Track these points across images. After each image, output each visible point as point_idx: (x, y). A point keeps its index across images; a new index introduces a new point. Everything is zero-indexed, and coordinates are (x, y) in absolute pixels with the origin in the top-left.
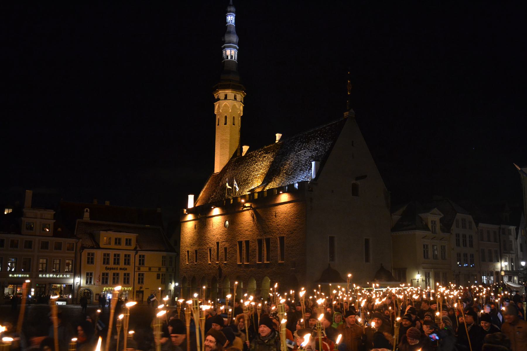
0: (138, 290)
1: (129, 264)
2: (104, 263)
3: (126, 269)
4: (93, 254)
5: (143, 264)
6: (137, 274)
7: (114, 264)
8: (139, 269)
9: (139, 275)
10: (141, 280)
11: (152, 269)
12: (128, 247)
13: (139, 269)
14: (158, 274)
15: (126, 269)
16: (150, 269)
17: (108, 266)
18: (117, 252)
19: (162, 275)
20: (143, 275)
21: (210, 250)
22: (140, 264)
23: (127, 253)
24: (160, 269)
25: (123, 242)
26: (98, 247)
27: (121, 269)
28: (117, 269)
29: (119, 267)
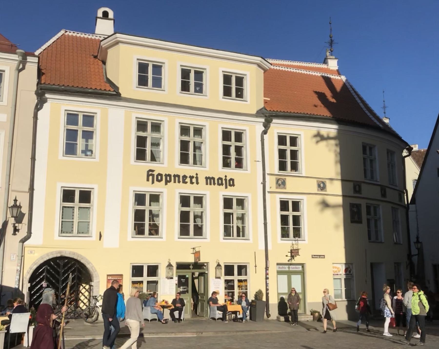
0: (285, 260)
1: (239, 164)
2: (141, 155)
3: (231, 183)
4: (89, 120)
5: (294, 167)
7: (184, 159)
8: (281, 183)
12: (232, 104)
13: (281, 183)
15: (231, 183)
17: (158, 168)
18: (192, 120)
22: (282, 166)
23: (233, 125)
27: (210, 180)
28: (194, 179)
29: (202, 172)
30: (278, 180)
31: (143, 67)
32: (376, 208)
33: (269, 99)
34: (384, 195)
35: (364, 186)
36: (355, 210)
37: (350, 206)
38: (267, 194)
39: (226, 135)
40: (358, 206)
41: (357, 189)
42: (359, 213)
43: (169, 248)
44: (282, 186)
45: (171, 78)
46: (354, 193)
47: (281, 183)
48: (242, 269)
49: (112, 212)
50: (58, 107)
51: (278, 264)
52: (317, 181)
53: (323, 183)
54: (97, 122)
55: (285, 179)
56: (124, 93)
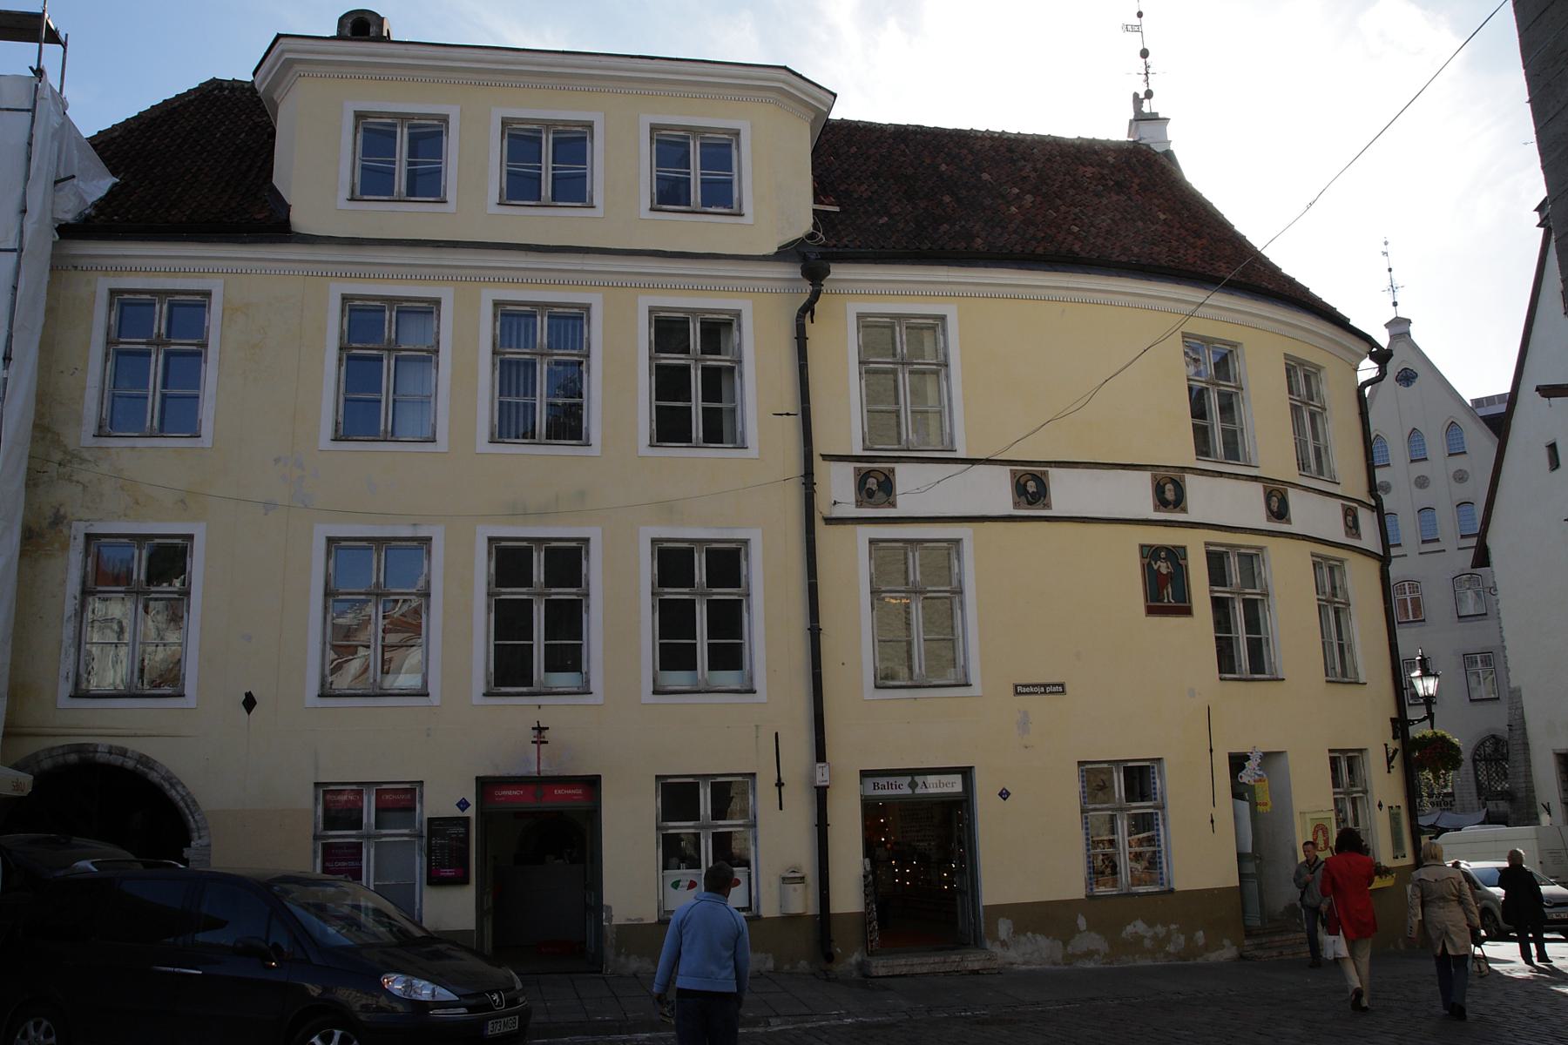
4: (189, 310)
11: (1067, 493)
13: (876, 485)
14: (1150, 553)
16: (1031, 487)
24: (1169, 490)
30: (862, 479)
32: (1250, 560)
33: (837, 209)
34: (1279, 511)
35: (1191, 482)
36: (1164, 567)
37: (1143, 557)
38: (819, 525)
40: (1176, 555)
41: (1170, 495)
42: (1179, 576)
43: (448, 731)
44: (880, 496)
46: (1156, 509)
47: (875, 487)
48: (726, 793)
51: (865, 774)
52: (1013, 473)
53: (1034, 477)
55: (892, 471)
56: (301, 220)
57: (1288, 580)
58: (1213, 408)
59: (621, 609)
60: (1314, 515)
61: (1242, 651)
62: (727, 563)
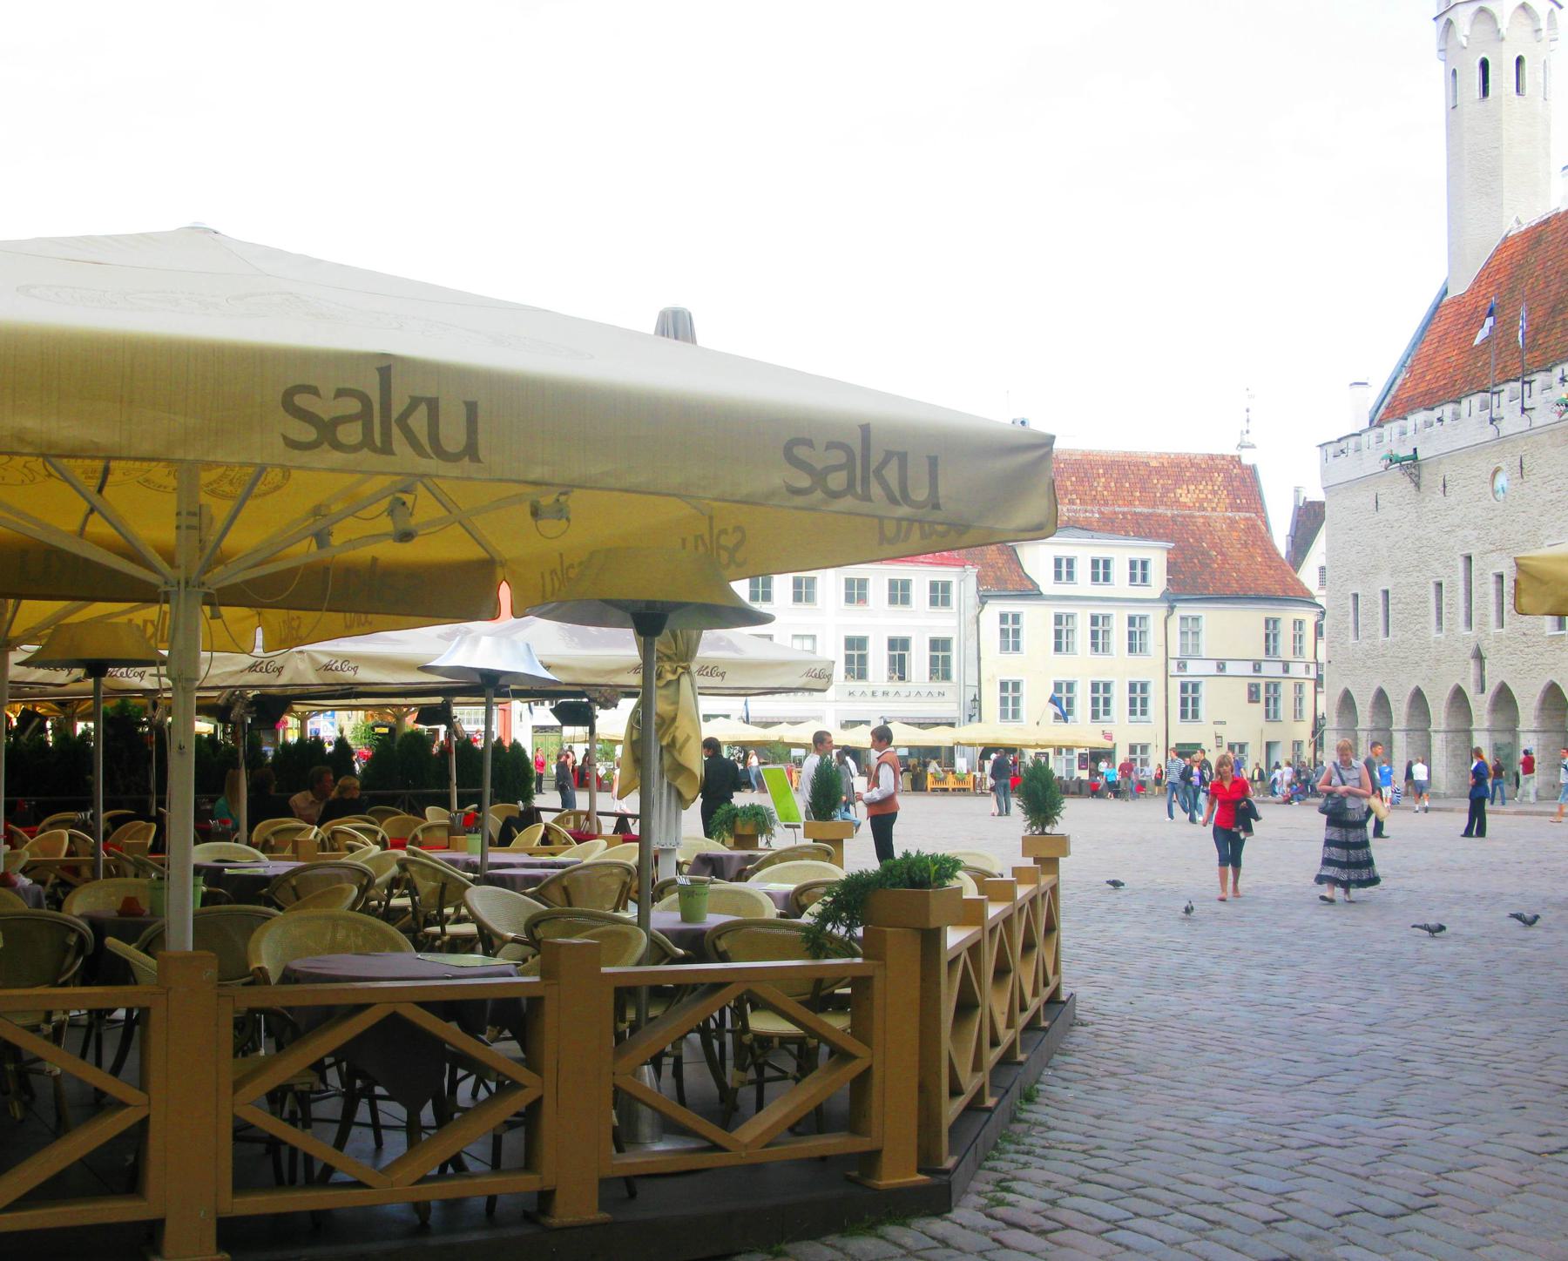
4: (1016, 618)
6: (1175, 685)
9: (1184, 687)
10: (1190, 708)
11: (1231, 668)
13: (1182, 666)
14: (1250, 685)
16: (1221, 666)
18: (1100, 611)
19: (1267, 685)
20: (1195, 687)
21: (1439, 585)
24: (1257, 666)
25: (1120, 571)
26: (1030, 592)
31: (1058, 562)
32: (1276, 686)
34: (1286, 670)
35: (1264, 665)
39: (1131, 621)
40: (1257, 686)
42: (1258, 691)
43: (1083, 732)
45: (1083, 570)
49: (1035, 700)
50: (994, 609)
54: (1024, 620)
56: (1045, 590)
57: (1287, 690)
58: (1271, 638)
59: (1120, 698)
60: (1297, 670)
61: (1271, 715)
62: (1144, 687)
